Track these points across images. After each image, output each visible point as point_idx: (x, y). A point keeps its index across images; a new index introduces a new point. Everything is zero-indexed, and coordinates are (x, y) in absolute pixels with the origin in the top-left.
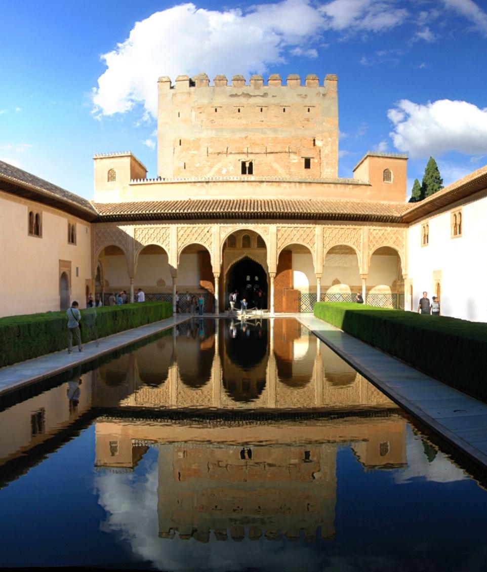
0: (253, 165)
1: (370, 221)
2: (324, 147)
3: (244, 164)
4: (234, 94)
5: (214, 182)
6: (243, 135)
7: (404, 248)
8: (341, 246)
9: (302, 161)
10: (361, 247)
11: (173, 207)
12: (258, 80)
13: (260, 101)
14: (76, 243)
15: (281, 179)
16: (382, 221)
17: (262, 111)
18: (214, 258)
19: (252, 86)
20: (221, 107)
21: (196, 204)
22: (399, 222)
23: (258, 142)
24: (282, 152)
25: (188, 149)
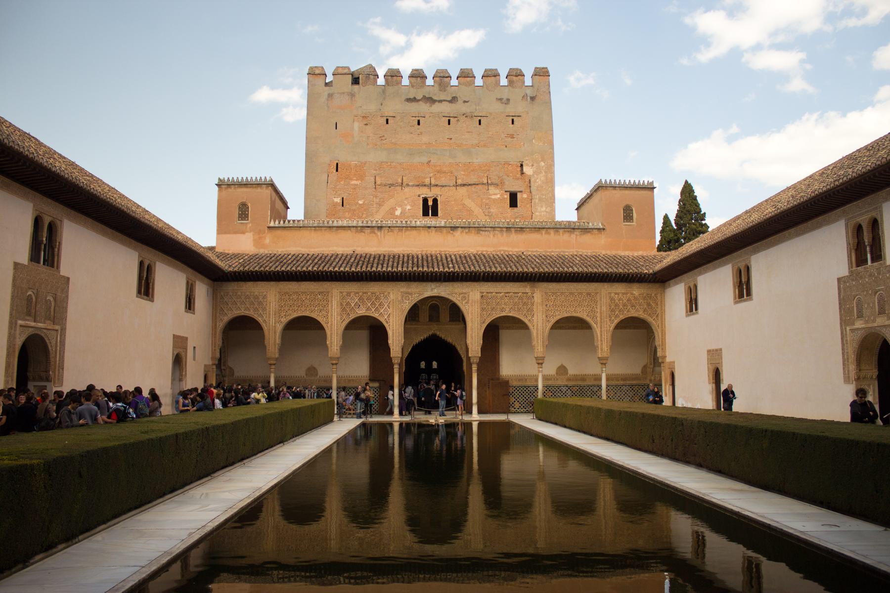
0: (439, 202)
2: (535, 176)
3: (425, 201)
4: (412, 97)
5: (389, 227)
6: (424, 159)
7: (659, 319)
8: (567, 318)
9: (506, 196)
10: (599, 319)
11: (335, 263)
13: (445, 108)
15: (481, 223)
17: (449, 124)
20: (394, 117)
22: (650, 282)
24: (478, 184)
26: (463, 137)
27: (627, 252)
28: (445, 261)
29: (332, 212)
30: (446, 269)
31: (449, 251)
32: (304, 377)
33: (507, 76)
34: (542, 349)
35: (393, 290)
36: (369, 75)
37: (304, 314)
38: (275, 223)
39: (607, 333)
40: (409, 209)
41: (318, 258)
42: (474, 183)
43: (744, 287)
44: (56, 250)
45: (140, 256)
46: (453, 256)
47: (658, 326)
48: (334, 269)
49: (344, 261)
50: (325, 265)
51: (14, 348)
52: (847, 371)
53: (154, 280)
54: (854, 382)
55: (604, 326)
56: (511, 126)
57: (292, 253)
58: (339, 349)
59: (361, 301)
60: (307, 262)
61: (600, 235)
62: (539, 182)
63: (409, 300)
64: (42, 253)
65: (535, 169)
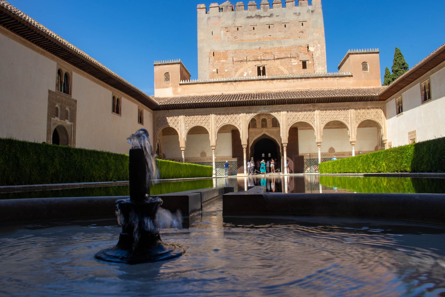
0: (266, 68)
1: (355, 101)
3: (259, 68)
4: (250, 16)
6: (257, 47)
9: (300, 63)
10: (350, 121)
11: (212, 99)
12: (266, 4)
13: (267, 20)
16: (363, 101)
17: (269, 28)
18: (242, 134)
22: (377, 100)
23: (268, 51)
24: (285, 58)
25: (219, 59)
26: (277, 34)
28: (268, 95)
30: (268, 99)
31: (270, 91)
34: (320, 138)
37: (197, 125)
39: (354, 129)
40: (251, 73)
42: (283, 57)
43: (427, 94)
44: (70, 86)
45: (113, 93)
47: (382, 124)
51: (50, 131)
53: (121, 107)
56: (302, 26)
57: (192, 96)
61: (350, 79)
62: (317, 55)
65: (315, 48)
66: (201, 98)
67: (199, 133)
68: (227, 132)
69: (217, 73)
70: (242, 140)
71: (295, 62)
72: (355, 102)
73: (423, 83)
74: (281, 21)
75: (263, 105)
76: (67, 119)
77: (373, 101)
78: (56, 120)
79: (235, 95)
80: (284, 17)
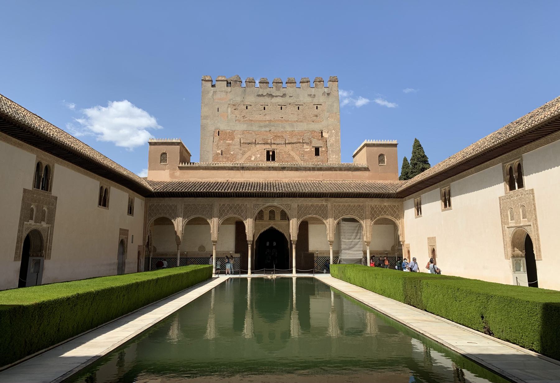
0: (275, 153)
1: (370, 197)
3: (268, 152)
4: (261, 94)
6: (268, 129)
9: (313, 150)
11: (216, 187)
12: (278, 83)
13: (280, 100)
14: (133, 214)
16: (380, 197)
17: (281, 109)
19: (274, 87)
21: (234, 185)
22: (394, 198)
23: (279, 135)
24: (297, 143)
27: (381, 181)
28: (277, 186)
29: (216, 157)
32: (197, 252)
33: (314, 82)
35: (248, 202)
36: (237, 81)
38: (182, 164)
39: (369, 227)
40: (259, 157)
41: (206, 184)
43: (447, 201)
44: (50, 181)
45: (100, 183)
46: (282, 184)
48: (215, 191)
49: (221, 186)
50: (210, 189)
52: (506, 252)
54: (511, 259)
55: (368, 223)
56: (316, 110)
57: (192, 181)
58: (217, 235)
59: (231, 208)
60: (200, 187)
63: (257, 208)
64: (41, 183)
66: (204, 184)
67: (199, 224)
68: (230, 224)
69: (222, 155)
70: (247, 235)
71: (308, 148)
72: (371, 199)
73: (443, 189)
74: (295, 103)
75: (272, 197)
76: (44, 221)
77: (390, 199)
78: (30, 224)
79: (242, 183)
80: (298, 98)
